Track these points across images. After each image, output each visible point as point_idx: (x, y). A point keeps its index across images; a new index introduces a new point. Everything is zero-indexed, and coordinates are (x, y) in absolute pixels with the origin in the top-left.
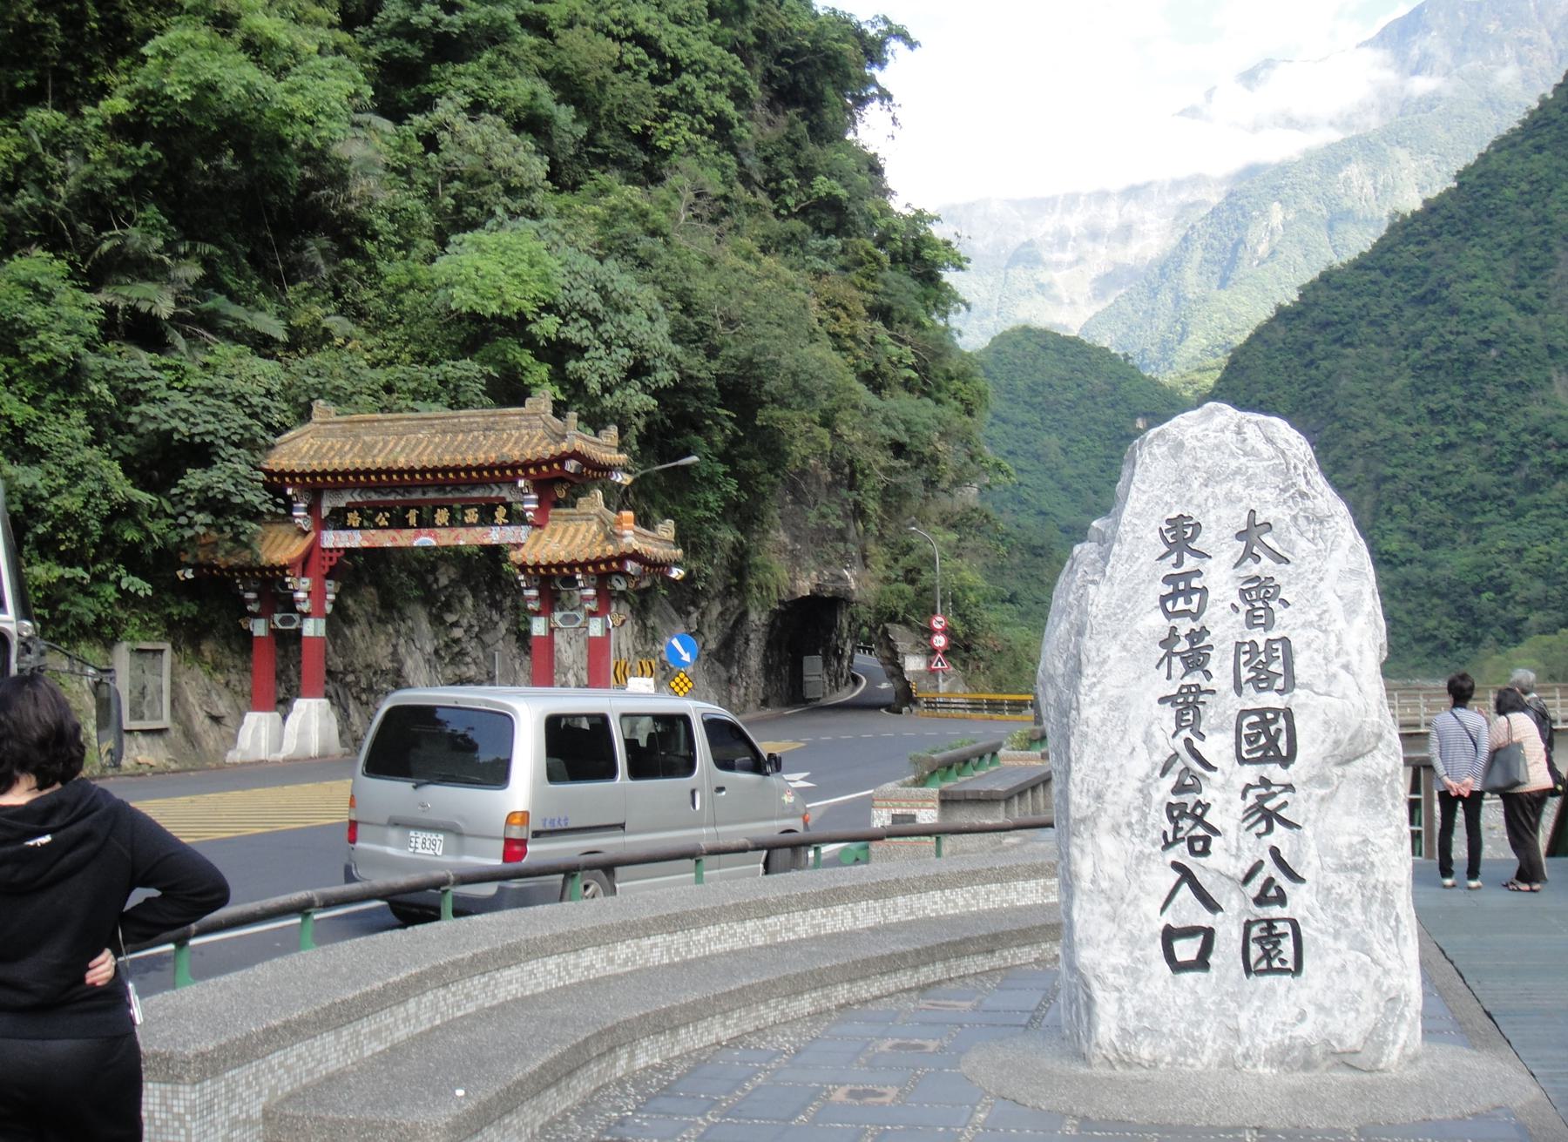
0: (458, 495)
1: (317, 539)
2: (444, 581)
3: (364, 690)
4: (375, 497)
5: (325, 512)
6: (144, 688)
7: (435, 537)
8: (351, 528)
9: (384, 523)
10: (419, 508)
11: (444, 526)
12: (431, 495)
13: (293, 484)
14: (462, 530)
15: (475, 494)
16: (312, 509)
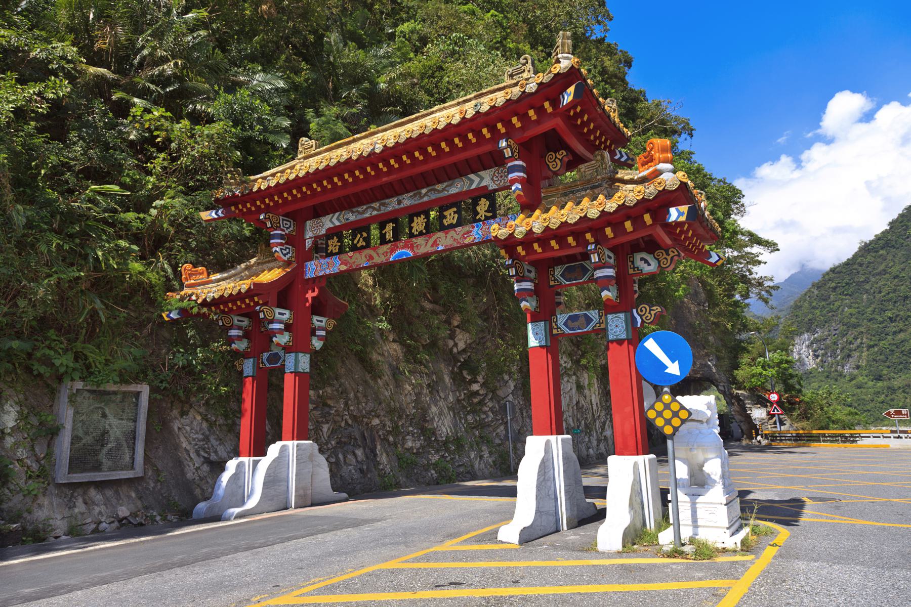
0: (434, 196)
1: (300, 270)
2: (461, 345)
3: (389, 432)
4: (352, 217)
5: (309, 243)
6: (105, 433)
7: (412, 248)
8: (331, 254)
9: (362, 243)
10: (395, 221)
11: (421, 234)
12: (407, 200)
13: (268, 209)
14: (441, 234)
15: (453, 191)
16: (295, 241)
